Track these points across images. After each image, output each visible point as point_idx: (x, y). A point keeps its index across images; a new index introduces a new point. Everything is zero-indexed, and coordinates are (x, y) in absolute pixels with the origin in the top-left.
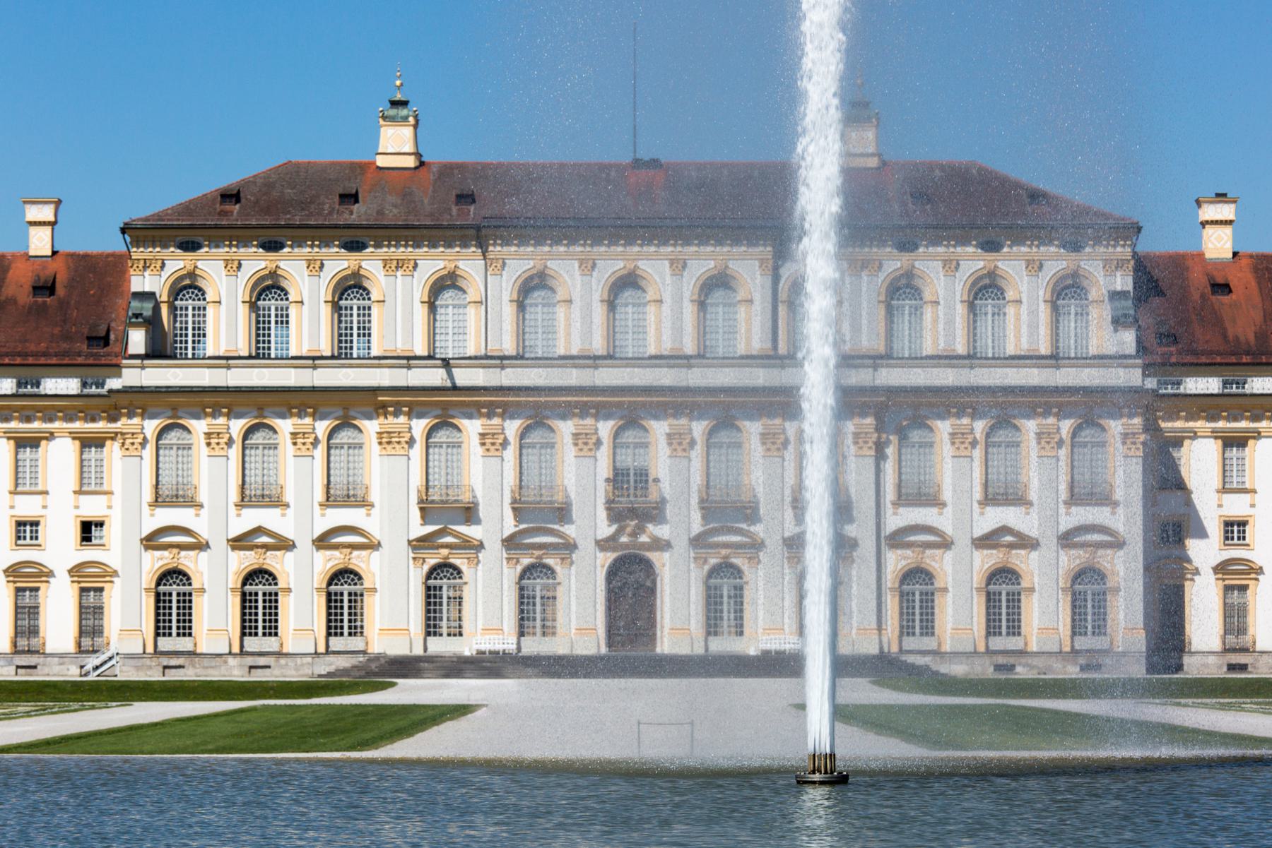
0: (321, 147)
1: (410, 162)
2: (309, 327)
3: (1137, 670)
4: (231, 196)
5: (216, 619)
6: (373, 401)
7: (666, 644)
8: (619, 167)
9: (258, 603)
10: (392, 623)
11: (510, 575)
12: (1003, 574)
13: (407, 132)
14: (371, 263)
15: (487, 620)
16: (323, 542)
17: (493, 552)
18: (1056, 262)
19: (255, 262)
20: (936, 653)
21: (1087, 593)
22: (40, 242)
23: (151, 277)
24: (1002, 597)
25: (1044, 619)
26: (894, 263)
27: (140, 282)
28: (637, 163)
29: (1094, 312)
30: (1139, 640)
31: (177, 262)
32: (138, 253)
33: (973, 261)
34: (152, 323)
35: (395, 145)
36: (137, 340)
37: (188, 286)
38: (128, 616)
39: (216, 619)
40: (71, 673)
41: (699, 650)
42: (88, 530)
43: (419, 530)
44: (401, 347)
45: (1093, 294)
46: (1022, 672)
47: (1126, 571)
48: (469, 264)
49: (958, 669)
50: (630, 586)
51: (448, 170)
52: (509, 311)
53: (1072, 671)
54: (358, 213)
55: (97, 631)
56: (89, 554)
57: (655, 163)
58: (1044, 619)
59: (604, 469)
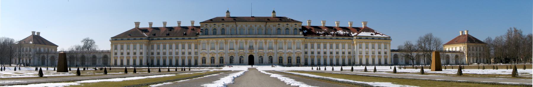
4: (211, 20)
59: (248, 46)
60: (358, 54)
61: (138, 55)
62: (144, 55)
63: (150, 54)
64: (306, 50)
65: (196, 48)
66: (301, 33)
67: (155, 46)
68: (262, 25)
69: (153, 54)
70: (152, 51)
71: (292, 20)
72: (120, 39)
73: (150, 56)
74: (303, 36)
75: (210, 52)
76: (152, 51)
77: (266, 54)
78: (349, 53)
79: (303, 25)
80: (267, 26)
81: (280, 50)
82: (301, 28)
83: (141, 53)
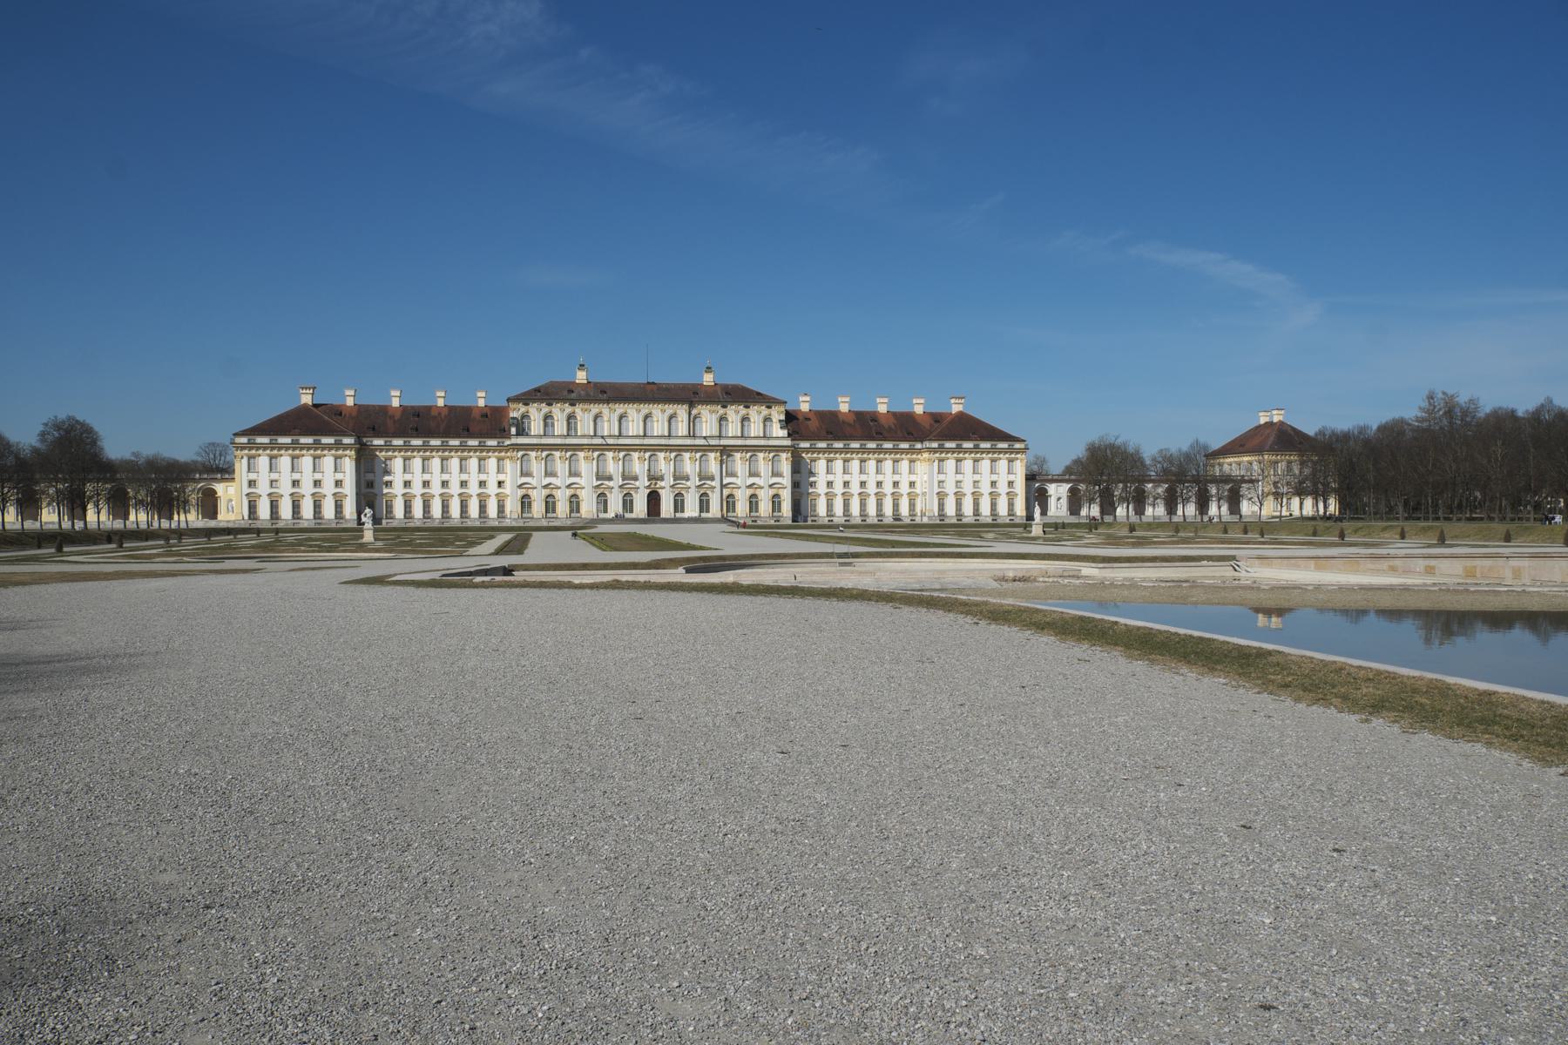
0: (560, 377)
2: (560, 427)
4: (537, 390)
6: (580, 447)
7: (664, 514)
12: (753, 496)
14: (578, 409)
16: (568, 486)
17: (616, 490)
18: (765, 411)
19: (545, 409)
21: (776, 501)
22: (481, 403)
23: (516, 412)
24: (753, 502)
25: (765, 508)
26: (722, 411)
27: (513, 414)
30: (790, 514)
31: (523, 409)
32: (512, 406)
33: (742, 410)
34: (518, 427)
35: (581, 377)
36: (513, 430)
38: (513, 507)
42: (500, 484)
48: (605, 409)
50: (654, 499)
54: (573, 395)
58: (765, 508)
60: (936, 490)
61: (328, 489)
62: (349, 489)
64: (797, 476)
66: (785, 433)
68: (682, 411)
70: (370, 477)
72: (265, 440)
73: (364, 490)
74: (788, 442)
75: (546, 481)
76: (370, 477)
77: (693, 490)
78: (912, 484)
80: (694, 412)
82: (783, 417)
83: (338, 483)
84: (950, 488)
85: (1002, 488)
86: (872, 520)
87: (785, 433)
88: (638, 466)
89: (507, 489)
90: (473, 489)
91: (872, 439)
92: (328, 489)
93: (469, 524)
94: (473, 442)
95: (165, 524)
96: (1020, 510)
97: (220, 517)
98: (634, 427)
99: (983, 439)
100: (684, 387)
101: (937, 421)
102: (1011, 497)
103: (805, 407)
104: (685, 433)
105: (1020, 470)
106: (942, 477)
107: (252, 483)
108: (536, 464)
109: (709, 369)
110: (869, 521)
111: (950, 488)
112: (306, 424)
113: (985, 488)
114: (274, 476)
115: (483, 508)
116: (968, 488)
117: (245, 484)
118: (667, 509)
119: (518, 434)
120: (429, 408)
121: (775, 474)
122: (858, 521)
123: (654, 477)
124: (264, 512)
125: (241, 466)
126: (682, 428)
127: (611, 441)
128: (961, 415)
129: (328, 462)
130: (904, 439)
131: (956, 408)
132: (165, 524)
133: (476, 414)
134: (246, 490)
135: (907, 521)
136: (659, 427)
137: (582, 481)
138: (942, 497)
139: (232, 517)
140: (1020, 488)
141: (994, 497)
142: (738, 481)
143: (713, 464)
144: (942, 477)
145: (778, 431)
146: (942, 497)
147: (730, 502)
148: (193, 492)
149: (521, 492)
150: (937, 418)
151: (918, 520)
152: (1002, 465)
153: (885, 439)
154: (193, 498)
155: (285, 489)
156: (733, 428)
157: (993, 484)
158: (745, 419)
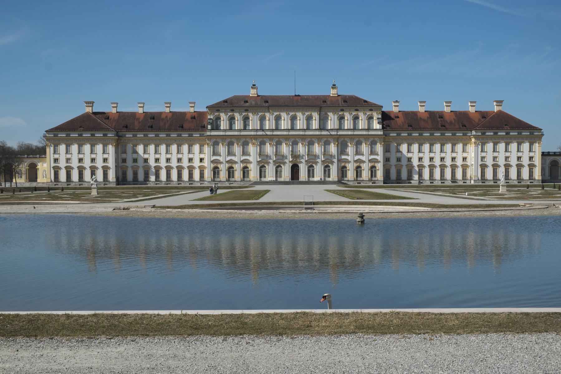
1: (256, 95)
2: (238, 125)
3: (382, 184)
4: (225, 101)
5: (223, 175)
8: (292, 96)
9: (231, 172)
10: (253, 175)
11: (274, 167)
12: (358, 167)
13: (256, 90)
15: (270, 176)
20: (348, 181)
22: (192, 110)
25: (365, 175)
27: (209, 117)
28: (296, 95)
29: (374, 121)
30: (382, 179)
34: (211, 124)
35: (253, 93)
37: (218, 118)
38: (208, 175)
39: (223, 175)
40: (199, 185)
41: (307, 180)
42: (201, 160)
43: (259, 160)
44: (255, 128)
45: (375, 118)
46: (362, 184)
47: (380, 167)
49: (351, 183)
50: (295, 169)
51: (262, 96)
52: (274, 122)
53: (371, 184)
54: (247, 104)
55: (203, 177)
56: (202, 164)
57: (299, 96)
58: (365, 175)
60: (480, 163)
61: (99, 163)
62: (111, 163)
63: (120, 161)
64: (388, 155)
65: (201, 152)
66: (381, 126)
67: (129, 147)
69: (124, 161)
70: (124, 156)
71: (365, 101)
72: (62, 135)
73: (121, 164)
76: (124, 156)
78: (464, 159)
79: (383, 109)
80: (323, 113)
81: (343, 157)
82: (380, 116)
83: (105, 160)
84: (489, 161)
85: (525, 161)
86: (438, 183)
87: (378, 126)
88: (285, 149)
89: (206, 163)
90: (185, 163)
91: (438, 129)
92: (99, 163)
93: (183, 185)
94: (185, 135)
95: (8, 185)
96: (537, 175)
97: (39, 180)
98: (285, 124)
99: (513, 128)
100: (317, 98)
101: (484, 117)
102: (531, 166)
103: (395, 110)
104: (317, 127)
105: (538, 149)
106: (483, 154)
107: (56, 160)
108: (222, 149)
109: (334, 86)
110: (435, 183)
111: (489, 161)
112: (87, 126)
113: (514, 162)
114: (69, 156)
115: (191, 175)
116: (501, 162)
117: (52, 161)
118: (303, 175)
119: (212, 129)
120: (160, 114)
121: (372, 153)
122: (428, 183)
123: (295, 156)
124: (63, 177)
125: (50, 150)
126: (315, 124)
127: (268, 133)
128: (500, 113)
129: (99, 148)
130: (460, 129)
131: (496, 109)
132: (8, 185)
133: (188, 117)
134: (53, 165)
135: (461, 183)
136: (300, 124)
137: (251, 159)
138: (484, 167)
139: (45, 180)
140: (537, 161)
141: (520, 167)
142: (349, 158)
143: (333, 149)
144: (483, 154)
145: (377, 125)
146: (484, 167)
147: (343, 171)
148: (24, 167)
149: (212, 166)
150: (483, 115)
151: (468, 183)
152: (526, 146)
153: (447, 129)
154: (24, 170)
155: (75, 164)
156: (348, 124)
157: (519, 158)
158: (356, 118)
